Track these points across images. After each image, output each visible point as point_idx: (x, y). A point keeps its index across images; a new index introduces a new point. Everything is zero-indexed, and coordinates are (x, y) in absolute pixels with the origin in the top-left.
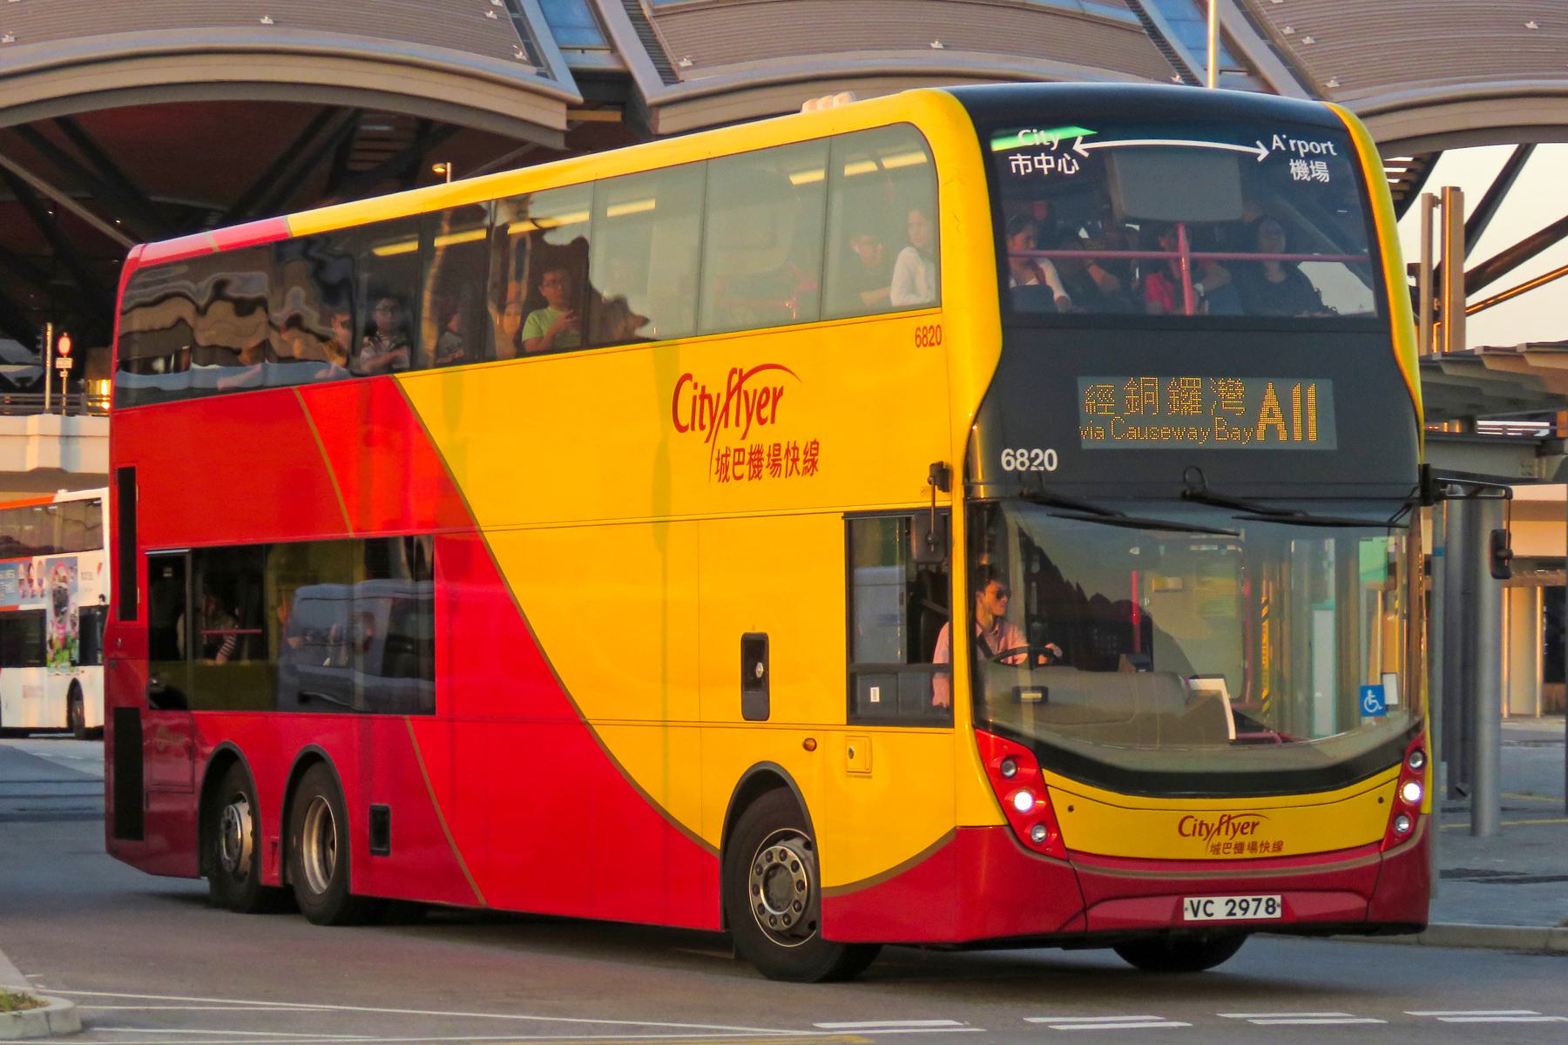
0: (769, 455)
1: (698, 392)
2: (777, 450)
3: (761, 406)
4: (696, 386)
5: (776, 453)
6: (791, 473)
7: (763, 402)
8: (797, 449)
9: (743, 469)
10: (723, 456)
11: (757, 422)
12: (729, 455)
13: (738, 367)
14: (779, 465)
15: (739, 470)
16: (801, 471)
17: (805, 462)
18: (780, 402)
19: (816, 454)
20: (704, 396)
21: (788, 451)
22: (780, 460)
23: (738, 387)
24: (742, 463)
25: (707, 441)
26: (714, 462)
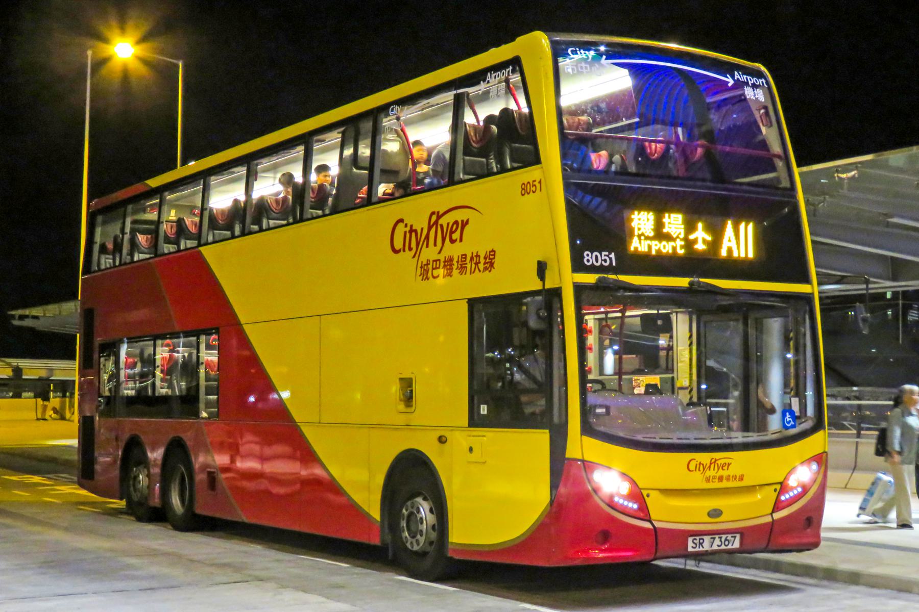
0: (458, 262)
1: (408, 229)
2: (464, 258)
3: (452, 232)
4: (406, 225)
5: (463, 260)
6: (474, 272)
7: (454, 229)
8: (479, 256)
9: (441, 272)
10: (425, 265)
11: (450, 243)
12: (429, 264)
13: (436, 210)
14: (466, 267)
15: (436, 273)
16: (482, 269)
17: (484, 264)
18: (467, 228)
19: (494, 258)
20: (411, 231)
21: (472, 259)
22: (466, 264)
23: (436, 223)
24: (439, 268)
25: (414, 257)
26: (419, 269)
